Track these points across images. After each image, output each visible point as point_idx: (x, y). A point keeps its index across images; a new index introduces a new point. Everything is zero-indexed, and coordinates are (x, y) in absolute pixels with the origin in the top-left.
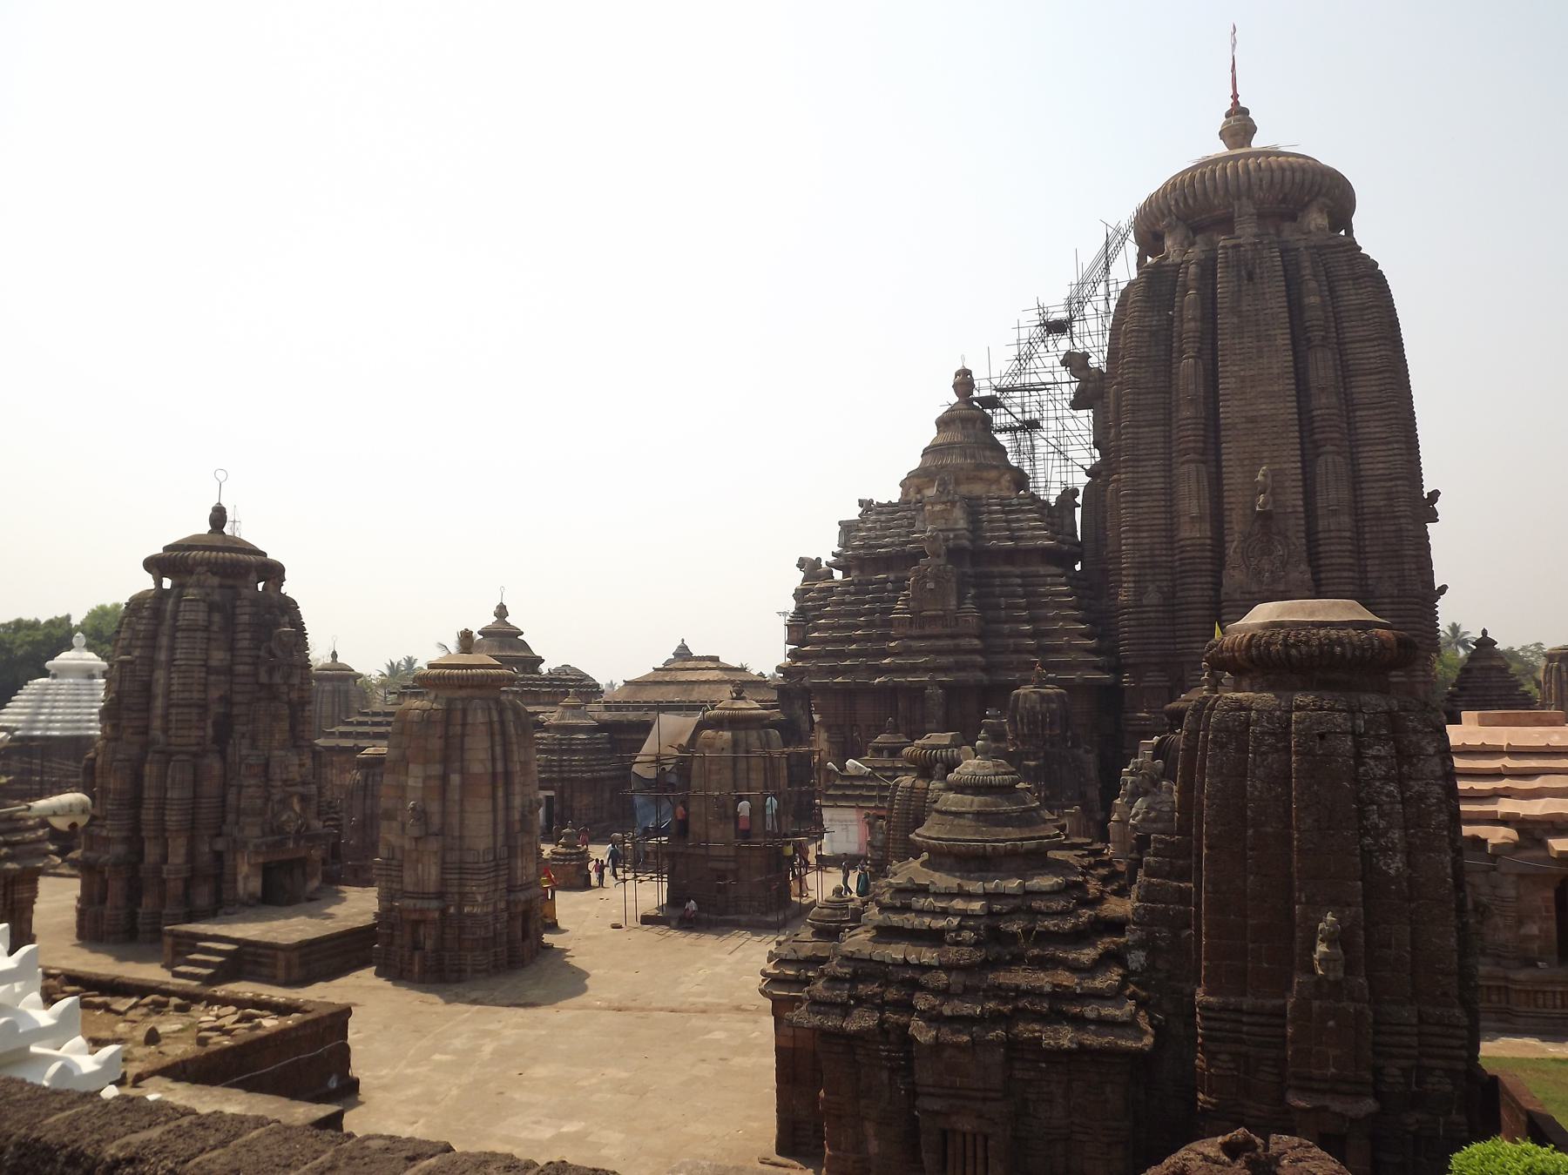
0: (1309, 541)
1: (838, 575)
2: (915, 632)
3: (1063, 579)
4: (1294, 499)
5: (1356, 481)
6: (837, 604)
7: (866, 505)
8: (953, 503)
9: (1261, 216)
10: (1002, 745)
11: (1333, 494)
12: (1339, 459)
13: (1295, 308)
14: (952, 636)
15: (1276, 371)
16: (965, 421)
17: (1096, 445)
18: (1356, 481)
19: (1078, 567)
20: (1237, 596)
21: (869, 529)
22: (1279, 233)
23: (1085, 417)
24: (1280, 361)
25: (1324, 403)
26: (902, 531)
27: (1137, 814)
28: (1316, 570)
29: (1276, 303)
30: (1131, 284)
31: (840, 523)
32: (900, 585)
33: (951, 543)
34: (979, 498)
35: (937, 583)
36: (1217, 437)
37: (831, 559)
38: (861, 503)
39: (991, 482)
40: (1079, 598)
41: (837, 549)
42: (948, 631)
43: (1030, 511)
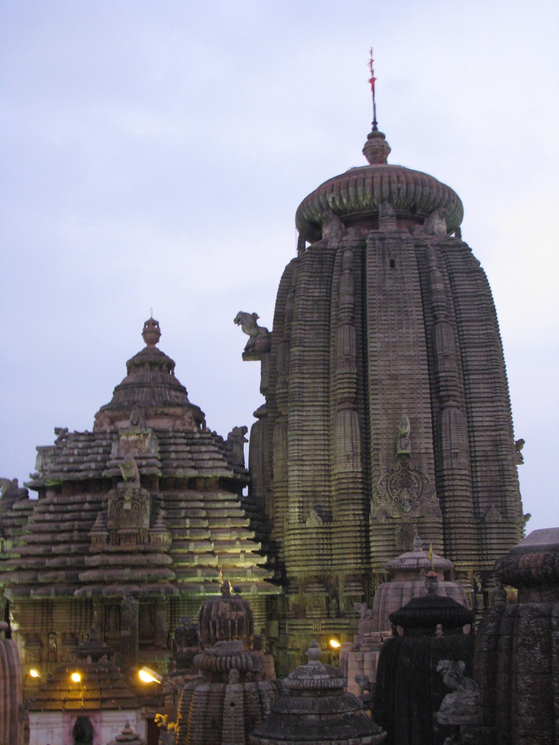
0: (436, 477)
1: (34, 495)
2: (111, 548)
3: (239, 504)
4: (426, 443)
5: (471, 430)
6: (37, 521)
7: (61, 433)
8: (146, 435)
9: (399, 217)
10: (194, 649)
11: (456, 439)
12: (458, 412)
13: (426, 291)
14: (145, 553)
15: (411, 339)
16: (152, 364)
17: (263, 390)
18: (471, 430)
19: (245, 492)
20: (383, 521)
21: (67, 455)
22: (411, 231)
23: (256, 366)
24: (414, 332)
25: (449, 368)
26: (99, 458)
27: (446, 709)
28: (443, 500)
29: (412, 286)
30: (293, 261)
31: (38, 448)
32: (97, 506)
33: (144, 471)
34: (167, 432)
35: (133, 505)
36: (366, 390)
37: (29, 480)
38: (57, 431)
39: (175, 417)
40: (252, 520)
41: (34, 471)
42: (142, 547)
43: (209, 444)
